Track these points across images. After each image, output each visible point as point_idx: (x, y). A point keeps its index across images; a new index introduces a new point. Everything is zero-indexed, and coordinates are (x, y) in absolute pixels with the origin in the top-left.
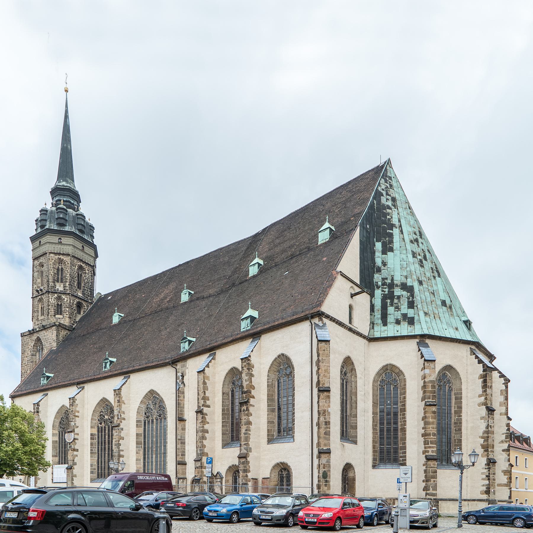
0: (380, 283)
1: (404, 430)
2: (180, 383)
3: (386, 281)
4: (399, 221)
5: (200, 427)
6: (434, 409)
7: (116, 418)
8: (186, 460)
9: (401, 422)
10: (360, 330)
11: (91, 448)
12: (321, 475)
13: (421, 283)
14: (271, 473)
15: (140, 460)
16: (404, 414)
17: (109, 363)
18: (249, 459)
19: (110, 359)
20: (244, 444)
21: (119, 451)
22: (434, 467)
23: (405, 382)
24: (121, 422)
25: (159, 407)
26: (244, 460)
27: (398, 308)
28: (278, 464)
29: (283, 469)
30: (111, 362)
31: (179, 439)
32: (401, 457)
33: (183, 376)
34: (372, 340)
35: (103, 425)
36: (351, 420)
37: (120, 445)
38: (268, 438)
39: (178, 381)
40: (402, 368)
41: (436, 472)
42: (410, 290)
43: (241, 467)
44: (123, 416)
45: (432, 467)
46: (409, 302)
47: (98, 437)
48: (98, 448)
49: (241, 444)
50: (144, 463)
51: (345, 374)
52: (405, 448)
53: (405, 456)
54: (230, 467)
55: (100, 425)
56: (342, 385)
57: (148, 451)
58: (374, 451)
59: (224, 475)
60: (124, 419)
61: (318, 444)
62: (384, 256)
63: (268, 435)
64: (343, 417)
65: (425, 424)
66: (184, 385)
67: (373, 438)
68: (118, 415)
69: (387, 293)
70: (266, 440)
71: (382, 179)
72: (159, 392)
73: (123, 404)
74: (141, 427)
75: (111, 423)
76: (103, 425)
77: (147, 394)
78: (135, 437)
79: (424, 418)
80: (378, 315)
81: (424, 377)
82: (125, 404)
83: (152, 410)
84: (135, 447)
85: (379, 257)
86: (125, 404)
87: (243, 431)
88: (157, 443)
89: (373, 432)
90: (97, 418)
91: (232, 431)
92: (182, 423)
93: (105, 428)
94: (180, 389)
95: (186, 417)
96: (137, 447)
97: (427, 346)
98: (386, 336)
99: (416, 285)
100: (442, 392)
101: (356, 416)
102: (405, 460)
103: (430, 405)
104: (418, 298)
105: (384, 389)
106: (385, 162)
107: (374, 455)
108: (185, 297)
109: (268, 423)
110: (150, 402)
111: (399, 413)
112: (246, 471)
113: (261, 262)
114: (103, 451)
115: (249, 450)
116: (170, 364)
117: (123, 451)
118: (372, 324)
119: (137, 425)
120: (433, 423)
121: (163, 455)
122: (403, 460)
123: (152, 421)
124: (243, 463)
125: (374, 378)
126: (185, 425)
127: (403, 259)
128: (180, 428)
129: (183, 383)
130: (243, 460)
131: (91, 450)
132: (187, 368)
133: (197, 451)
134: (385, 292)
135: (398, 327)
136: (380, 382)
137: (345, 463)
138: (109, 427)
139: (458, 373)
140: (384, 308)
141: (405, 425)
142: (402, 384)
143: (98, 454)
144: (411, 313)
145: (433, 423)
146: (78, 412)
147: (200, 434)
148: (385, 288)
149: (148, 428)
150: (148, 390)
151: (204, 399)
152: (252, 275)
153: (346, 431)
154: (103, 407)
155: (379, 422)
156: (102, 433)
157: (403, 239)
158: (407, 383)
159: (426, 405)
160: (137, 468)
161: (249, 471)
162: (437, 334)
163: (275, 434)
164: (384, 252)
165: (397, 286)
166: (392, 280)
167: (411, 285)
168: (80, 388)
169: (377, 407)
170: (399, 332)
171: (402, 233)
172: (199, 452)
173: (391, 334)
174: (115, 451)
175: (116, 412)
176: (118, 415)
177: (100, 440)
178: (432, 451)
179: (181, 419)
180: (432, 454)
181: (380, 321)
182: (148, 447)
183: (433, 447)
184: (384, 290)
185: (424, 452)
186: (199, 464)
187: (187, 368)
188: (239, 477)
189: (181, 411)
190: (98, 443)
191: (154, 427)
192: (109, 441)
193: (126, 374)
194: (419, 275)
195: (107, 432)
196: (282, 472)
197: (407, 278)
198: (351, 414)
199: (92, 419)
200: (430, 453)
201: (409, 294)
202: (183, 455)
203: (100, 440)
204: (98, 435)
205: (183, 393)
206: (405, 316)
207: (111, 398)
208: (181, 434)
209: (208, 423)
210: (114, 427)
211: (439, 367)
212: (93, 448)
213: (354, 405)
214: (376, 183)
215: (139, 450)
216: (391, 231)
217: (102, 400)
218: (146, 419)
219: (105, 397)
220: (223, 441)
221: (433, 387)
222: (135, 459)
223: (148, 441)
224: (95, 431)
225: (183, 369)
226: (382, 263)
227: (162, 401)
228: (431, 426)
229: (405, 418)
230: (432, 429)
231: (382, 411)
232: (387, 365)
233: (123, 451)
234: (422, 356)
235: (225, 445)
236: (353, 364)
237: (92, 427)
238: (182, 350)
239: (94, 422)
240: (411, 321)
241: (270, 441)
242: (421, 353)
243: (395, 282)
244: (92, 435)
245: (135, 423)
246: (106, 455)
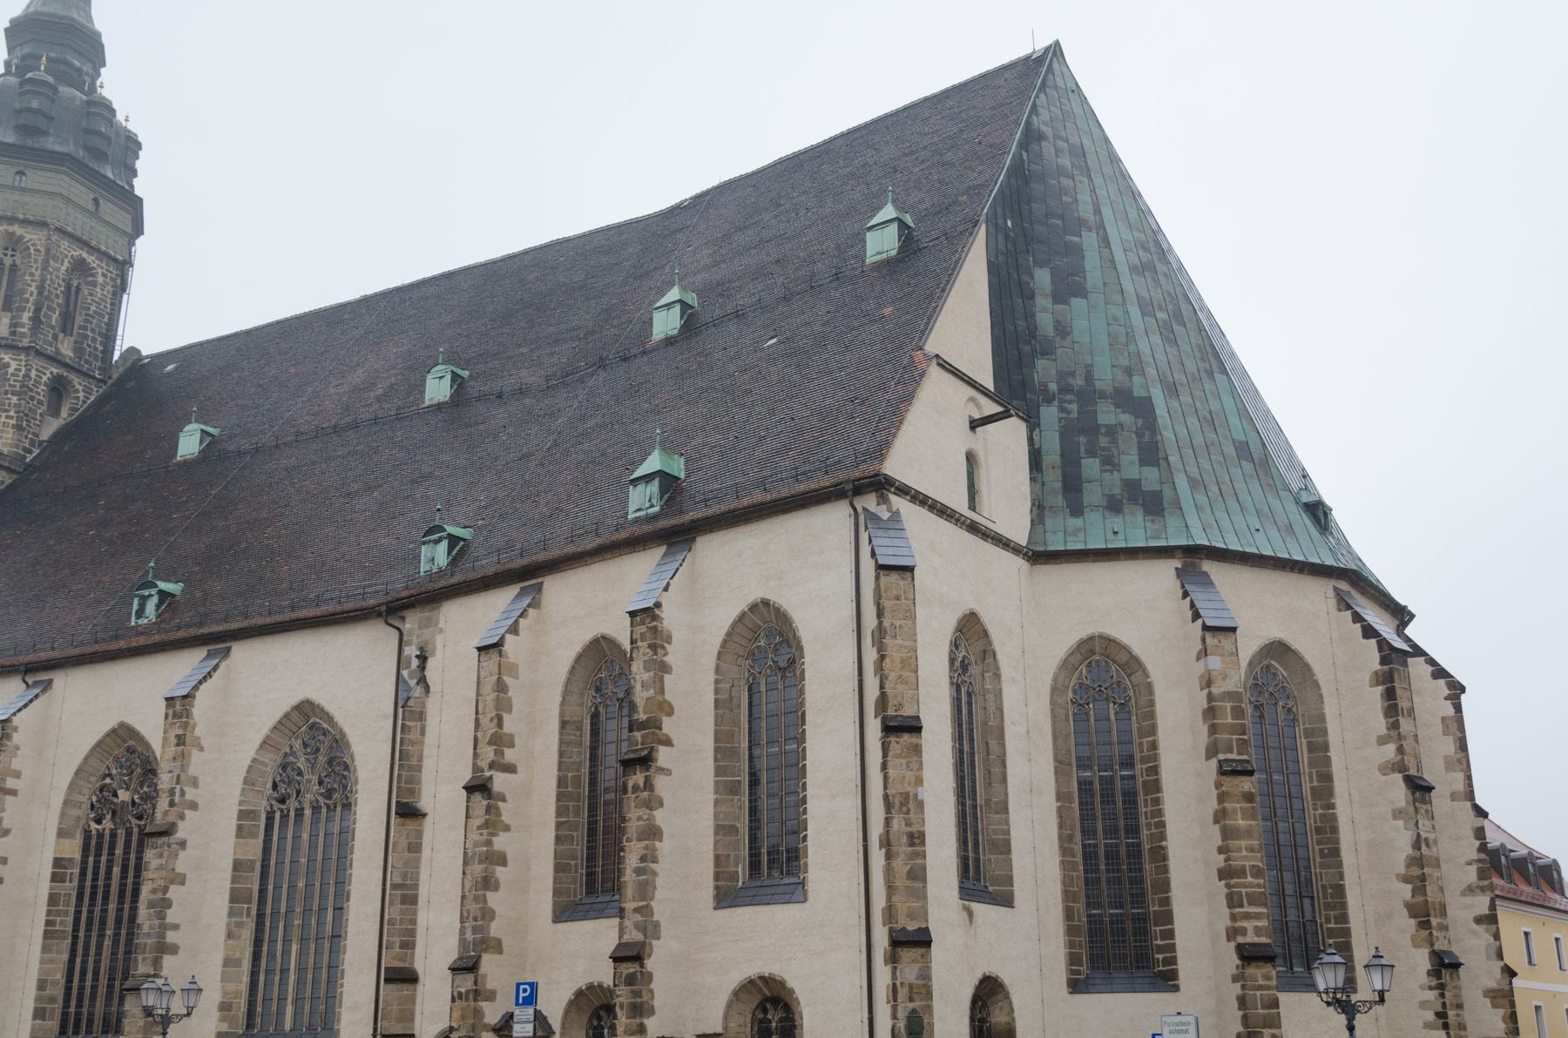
0: (1053, 387)
1: (1160, 855)
2: (412, 683)
3: (1071, 380)
4: (1098, 211)
5: (476, 844)
6: (1246, 784)
7: (163, 803)
8: (418, 966)
9: (1148, 826)
10: (1001, 528)
11: (49, 913)
12: (901, 1025)
13: (1172, 390)
14: (726, 1017)
15: (237, 963)
16: (1157, 801)
17: (155, 599)
18: (650, 964)
19: (162, 585)
20: (636, 910)
21: (164, 927)
22: (1268, 988)
23: (1151, 692)
24: (182, 817)
25: (330, 762)
26: (631, 968)
27: (1110, 463)
28: (751, 982)
29: (767, 999)
30: (163, 595)
31: (395, 886)
32: (1160, 949)
33: (423, 658)
34: (1039, 557)
35: (107, 824)
36: (989, 823)
37: (167, 904)
38: (717, 888)
39: (405, 673)
40: (1137, 650)
41: (1275, 1004)
42: (1143, 409)
43: (623, 997)
44: (191, 794)
45: (1261, 988)
46: (1142, 448)
47: (83, 873)
48: (78, 913)
49: (622, 910)
50: (254, 974)
51: (965, 667)
52: (1167, 917)
53: (1172, 948)
54: (580, 994)
55: (94, 826)
56: (957, 702)
57: (274, 928)
58: (1071, 930)
60: (193, 806)
61: (890, 912)
62: (1060, 307)
63: (717, 877)
64: (964, 811)
65: (1224, 838)
66: (427, 689)
67: (1064, 883)
68: (172, 792)
69: (1075, 415)
70: (711, 892)
71: (1042, 96)
72: (331, 709)
73: (194, 752)
74: (255, 836)
75: (140, 818)
76: (107, 824)
77: (287, 716)
78: (228, 875)
79: (1220, 816)
80: (1053, 478)
81: (1208, 682)
82: (201, 749)
83: (300, 773)
84: (225, 911)
85: (1045, 310)
86: (201, 749)
87: (632, 860)
88: (308, 897)
89: (1063, 862)
90: (85, 797)
91: (591, 857)
92: (411, 825)
93: (113, 835)
94: (411, 703)
95: (425, 803)
96: (231, 914)
97: (1206, 581)
98: (1081, 546)
99: (1157, 395)
100: (1268, 730)
101: (1004, 808)
102: (1173, 960)
103: (1235, 773)
104: (1168, 434)
105: (1087, 714)
106: (1047, 49)
107: (1071, 944)
108: (438, 389)
109: (716, 833)
110: (297, 744)
111: (1141, 797)
112: (640, 1009)
113: (692, 299)
114: (96, 927)
115: (651, 929)
116: (379, 615)
117: (175, 927)
118: (1039, 510)
119: (240, 828)
120: (1249, 833)
121: (327, 945)
122: (1167, 962)
123: (299, 813)
124: (630, 980)
125: (1055, 679)
126: (420, 833)
127: (1115, 319)
128: (403, 842)
129: (422, 681)
130: (628, 969)
131: (48, 923)
132: (441, 631)
133: (462, 931)
134: (1069, 412)
135: (1116, 522)
136: (1075, 692)
137: (979, 975)
138: (129, 834)
139: (1307, 668)
140: (1070, 462)
141: (1163, 837)
142: (1143, 700)
143: (75, 937)
144: (1150, 478)
145: (1249, 833)
146: (17, 775)
147: (478, 868)
148: (1071, 402)
149: (282, 838)
150: (294, 701)
151: (493, 740)
152: (662, 336)
153: (977, 860)
154: (117, 760)
155: (1078, 825)
156: (98, 855)
157: (1112, 262)
158: (1158, 699)
159: (1222, 772)
160: (225, 993)
161: (652, 1012)
162: (1235, 546)
163: (742, 871)
164: (1059, 297)
165: (1103, 395)
166: (1089, 378)
167: (1143, 393)
168: (36, 684)
169: (1069, 774)
170: (1121, 536)
171: (1108, 245)
172: (469, 936)
173: (1096, 544)
174: (145, 929)
175: (165, 780)
176: (172, 792)
177: (88, 883)
178: (1258, 931)
179: (407, 811)
180: (1257, 940)
181: (1060, 501)
182: (275, 913)
183: (1257, 916)
184: (1070, 407)
185: (1232, 933)
186: (466, 983)
187: (441, 631)
188: (613, 1028)
189: (410, 781)
191: (305, 836)
192: (123, 886)
193: (218, 641)
194: (1164, 366)
195: (119, 851)
196: (765, 1011)
197: (1130, 376)
198: (988, 801)
199: (66, 802)
200: (1251, 938)
201: (1140, 422)
202: (408, 945)
203: (88, 883)
204: (84, 863)
205: (421, 716)
206: (1133, 489)
207: (152, 727)
208: (407, 863)
209: (507, 828)
210: (152, 835)
211: (1248, 646)
212: (58, 913)
213: (996, 770)
214: (1022, 104)
215: (239, 925)
216: (1076, 239)
217: (114, 731)
218: (276, 806)
219: (130, 721)
220: (556, 893)
221: (1238, 712)
222: (218, 958)
223: (277, 887)
225: (427, 632)
226: (1056, 329)
227: (339, 742)
228: (1243, 843)
229: (1160, 813)
230: (1249, 854)
231: (1085, 786)
232: (1091, 638)
233: (175, 927)
234: (1196, 616)
235: (565, 911)
236: (986, 634)
237: (62, 834)
238: (424, 567)
239: (75, 812)
240: (1154, 505)
241: (726, 897)
242: (1192, 605)
243: (1097, 383)
244: (58, 862)
245: (234, 822)
246: (107, 943)
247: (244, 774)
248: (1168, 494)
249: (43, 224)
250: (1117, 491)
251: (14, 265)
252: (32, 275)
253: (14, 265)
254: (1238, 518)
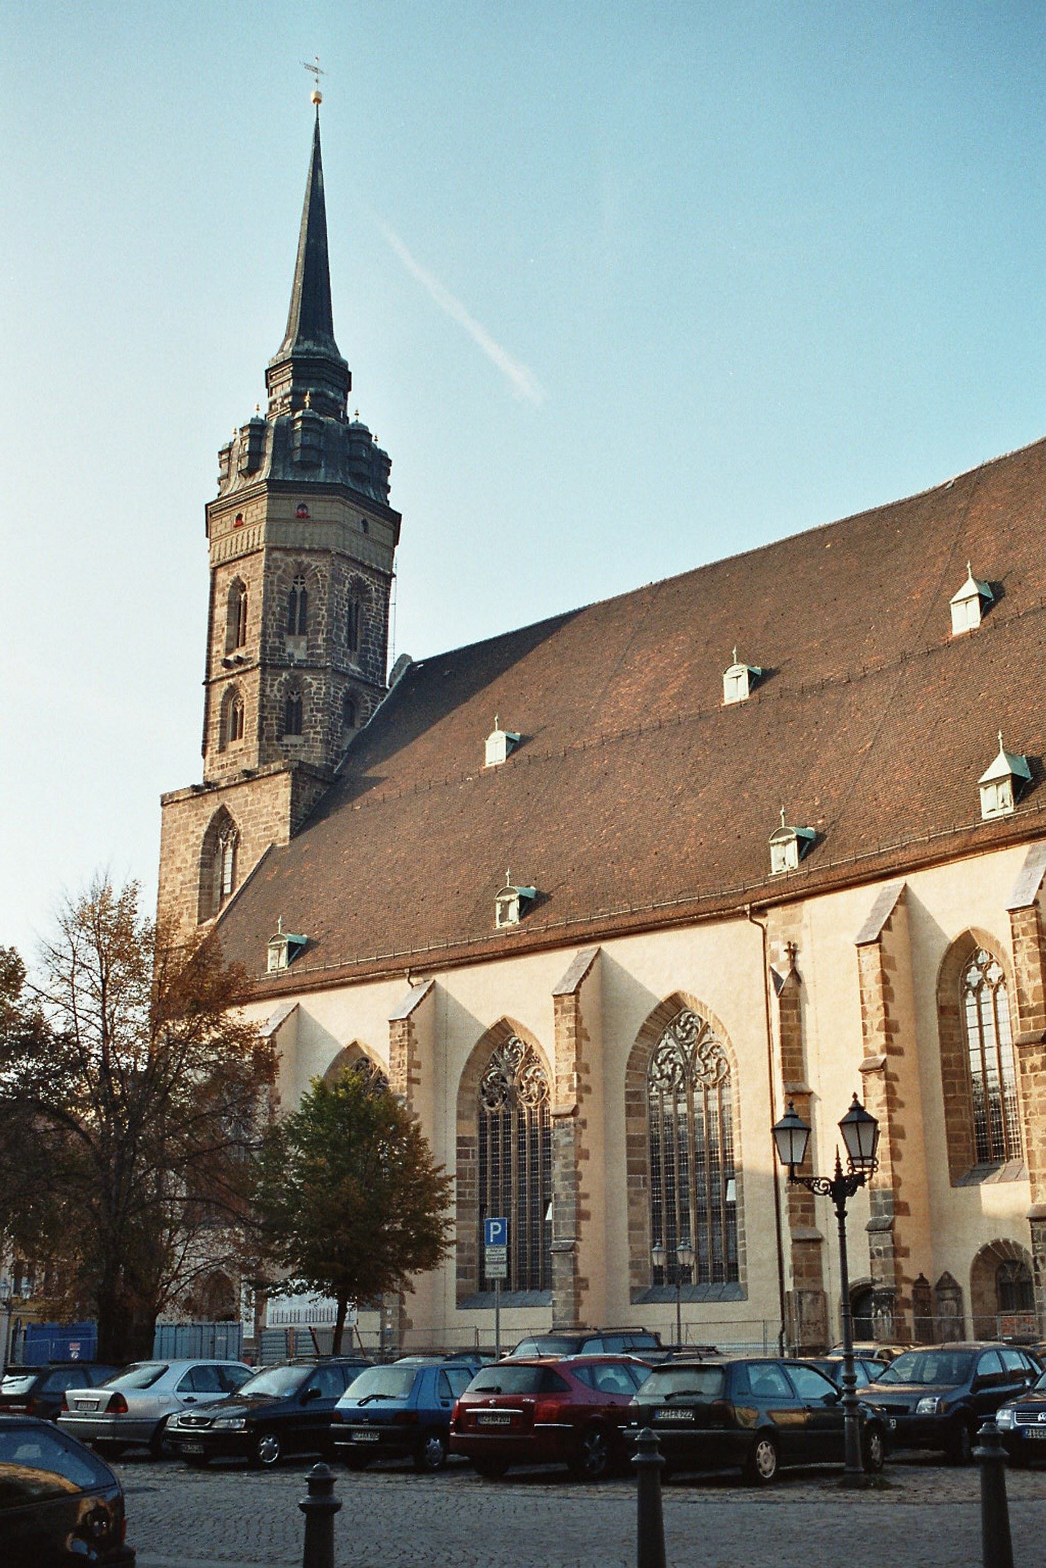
47: (483, 1149)
55: (487, 1108)
59: (963, 1279)
76: (500, 1106)
190: (483, 1171)
204: (483, 1140)
212: (467, 1185)
224: (472, 1131)
238: (776, 867)
239: (470, 1097)
244: (461, 1141)
247: (627, 1060)
249: (326, 551)
251: (304, 592)
252: (321, 599)
253: (304, 592)
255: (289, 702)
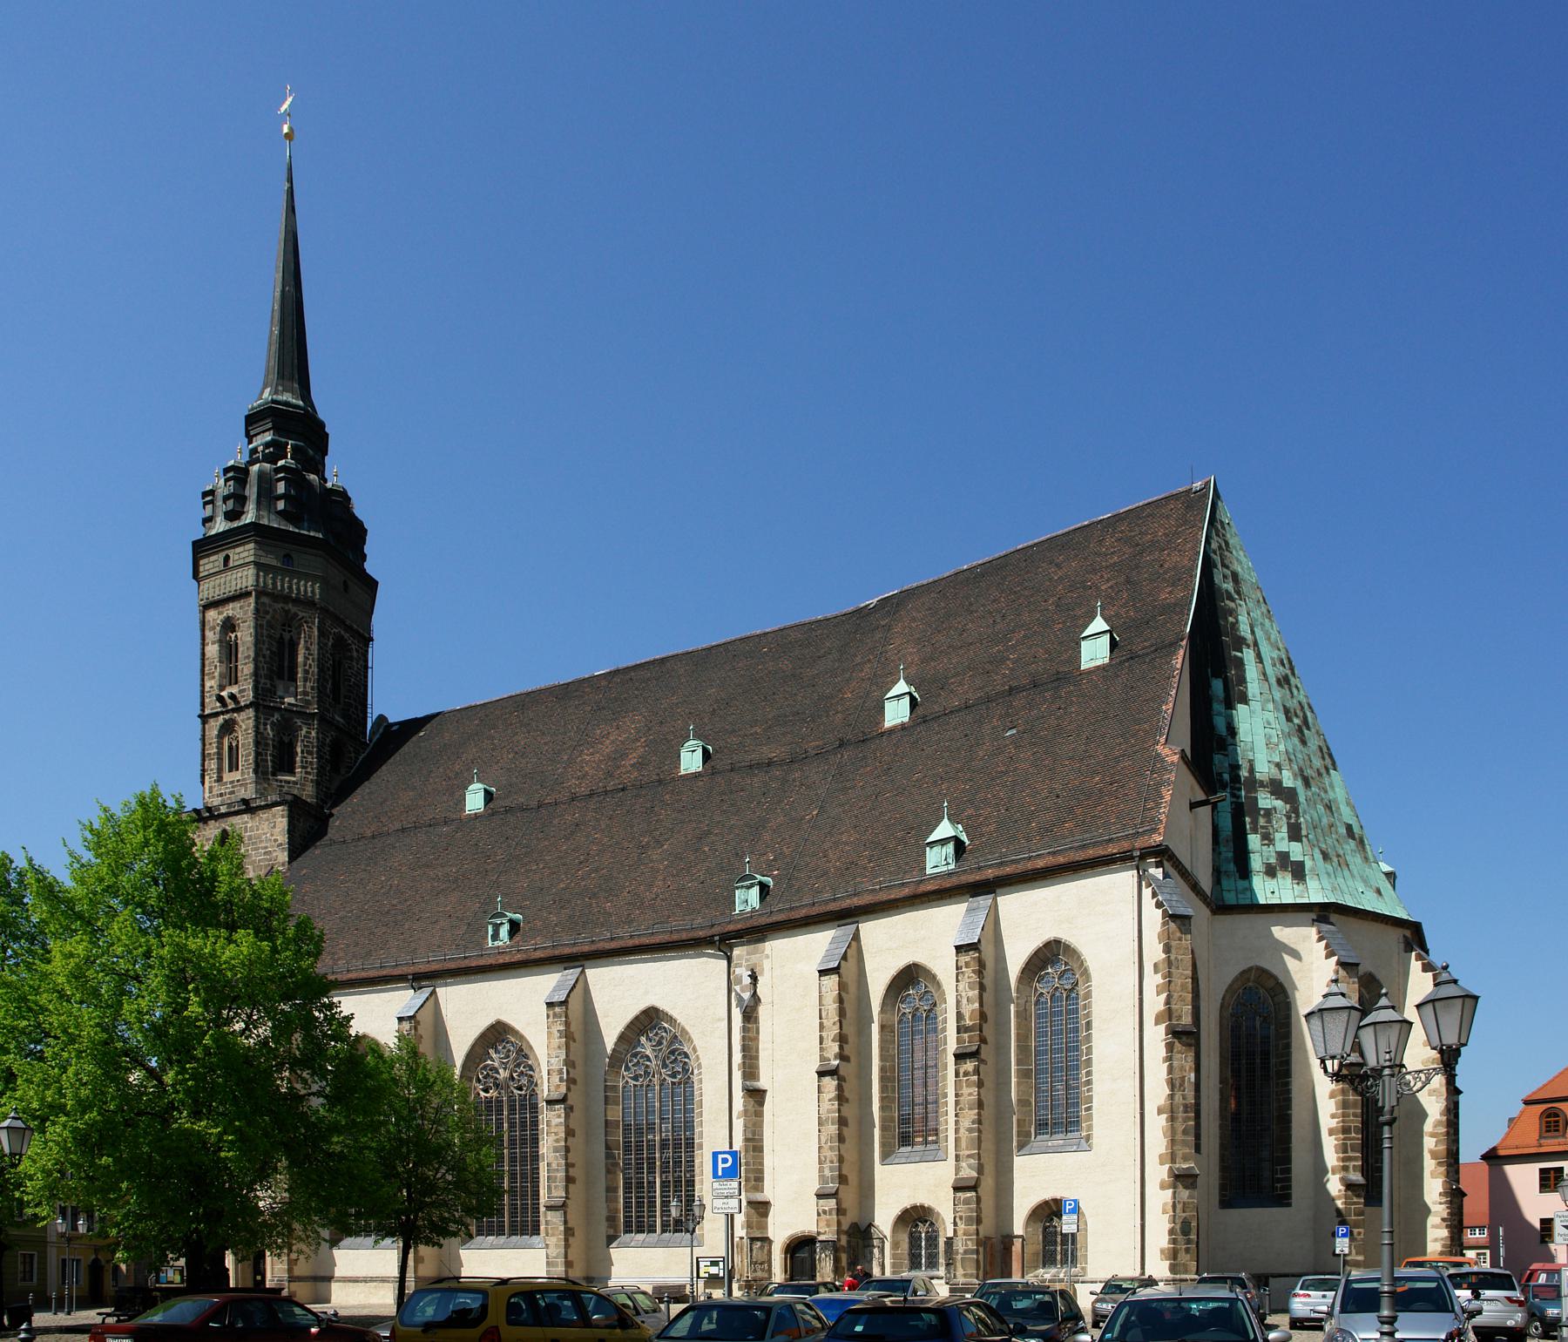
27: (1268, 838)
144: (1296, 851)
206: (1283, 857)
240: (1298, 872)
248: (1308, 864)
250: (1273, 861)
254: (1350, 882)
255: (281, 742)
